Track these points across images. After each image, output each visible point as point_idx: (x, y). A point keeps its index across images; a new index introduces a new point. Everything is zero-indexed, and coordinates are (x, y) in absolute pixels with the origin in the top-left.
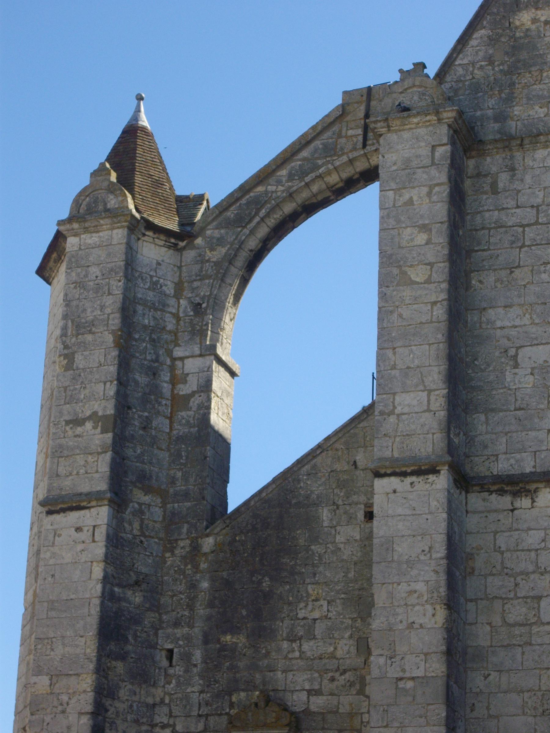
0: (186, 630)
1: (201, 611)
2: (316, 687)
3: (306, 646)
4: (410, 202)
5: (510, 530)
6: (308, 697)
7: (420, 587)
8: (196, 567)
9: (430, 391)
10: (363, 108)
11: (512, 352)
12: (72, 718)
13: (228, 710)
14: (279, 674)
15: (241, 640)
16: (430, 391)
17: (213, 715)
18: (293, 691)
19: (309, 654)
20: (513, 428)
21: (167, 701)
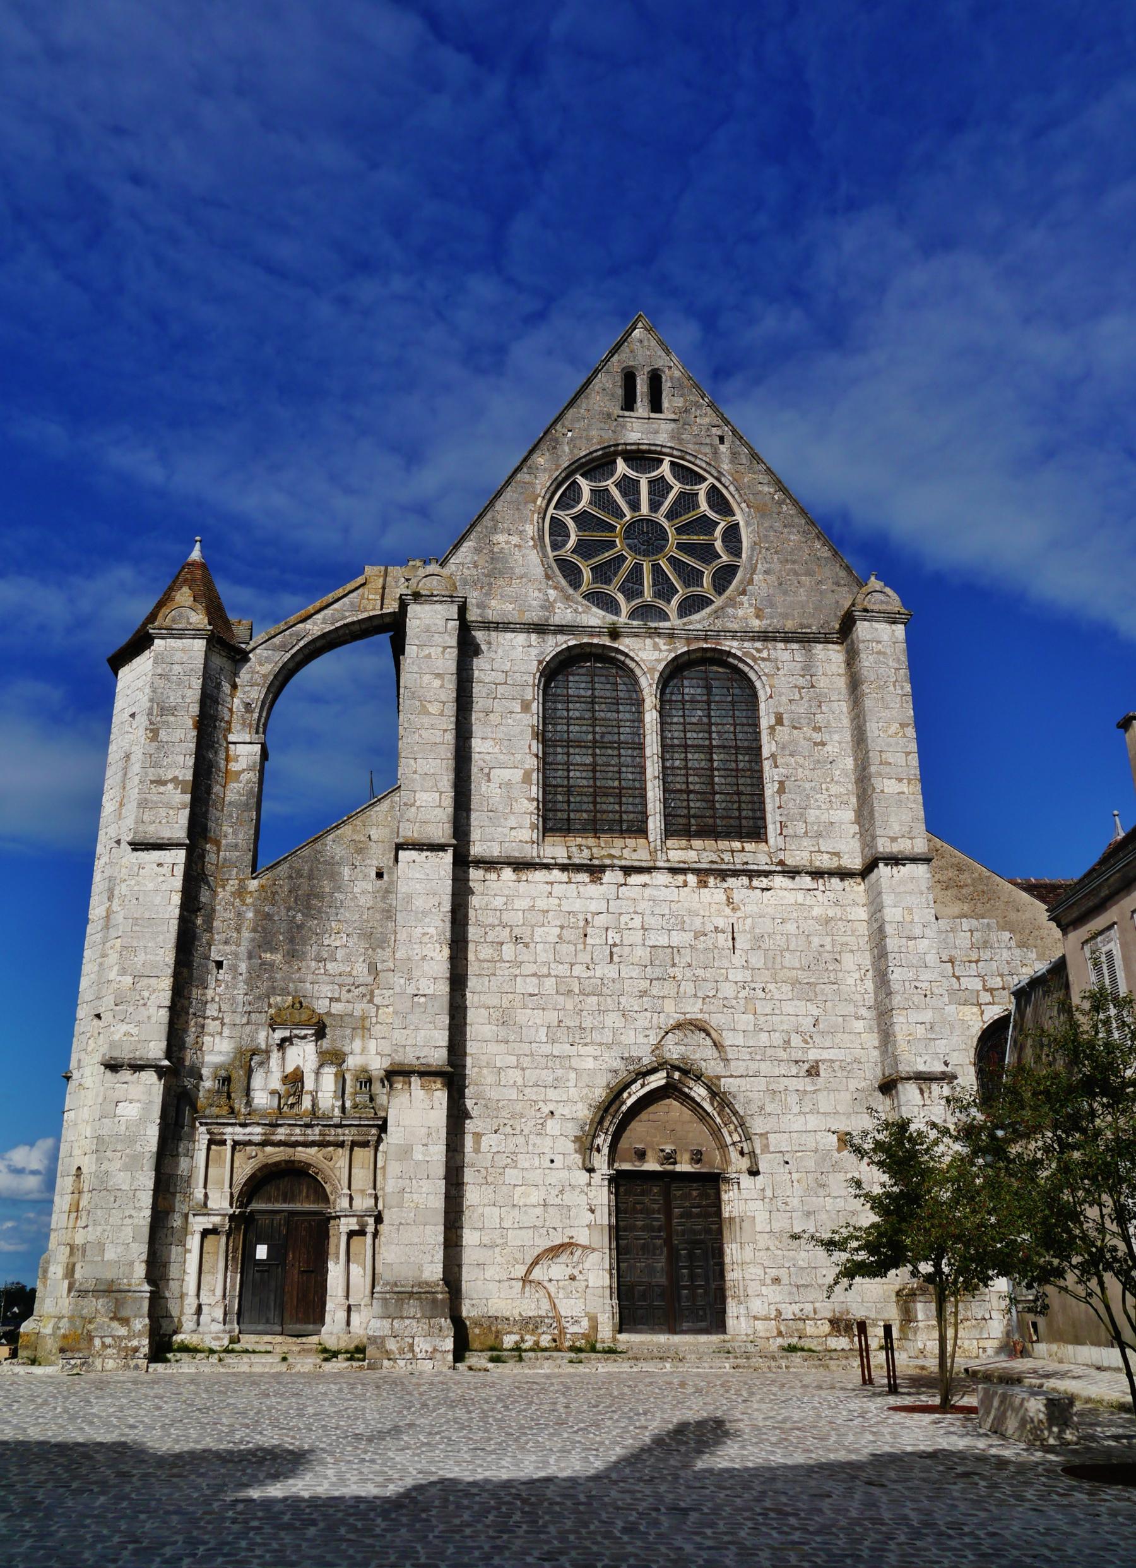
0: (234, 947)
1: (246, 934)
2: (337, 996)
3: (329, 966)
4: (429, 656)
5: (482, 894)
7: (432, 931)
8: (244, 903)
9: (441, 793)
10: (381, 580)
11: (486, 771)
12: (153, 1010)
14: (308, 985)
15: (278, 957)
16: (441, 793)
19: (331, 972)
20: (486, 824)
21: (217, 999)
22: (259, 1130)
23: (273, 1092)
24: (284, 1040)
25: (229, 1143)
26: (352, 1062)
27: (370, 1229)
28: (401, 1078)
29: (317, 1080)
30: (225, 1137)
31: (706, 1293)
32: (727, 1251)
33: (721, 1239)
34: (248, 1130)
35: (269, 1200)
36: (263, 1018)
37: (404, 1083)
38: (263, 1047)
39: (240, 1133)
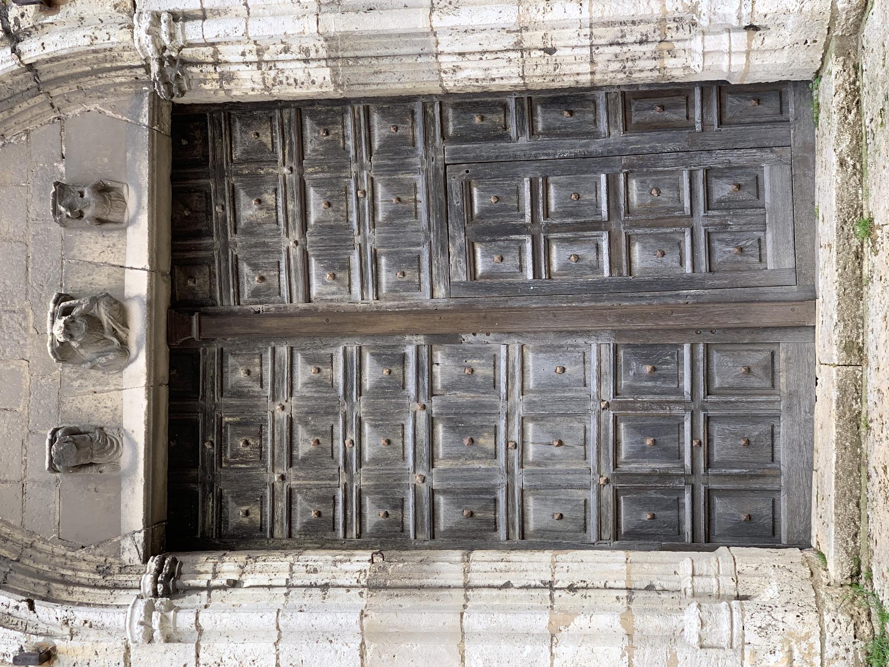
31: (641, 166)
32: (468, 75)
33: (427, 100)
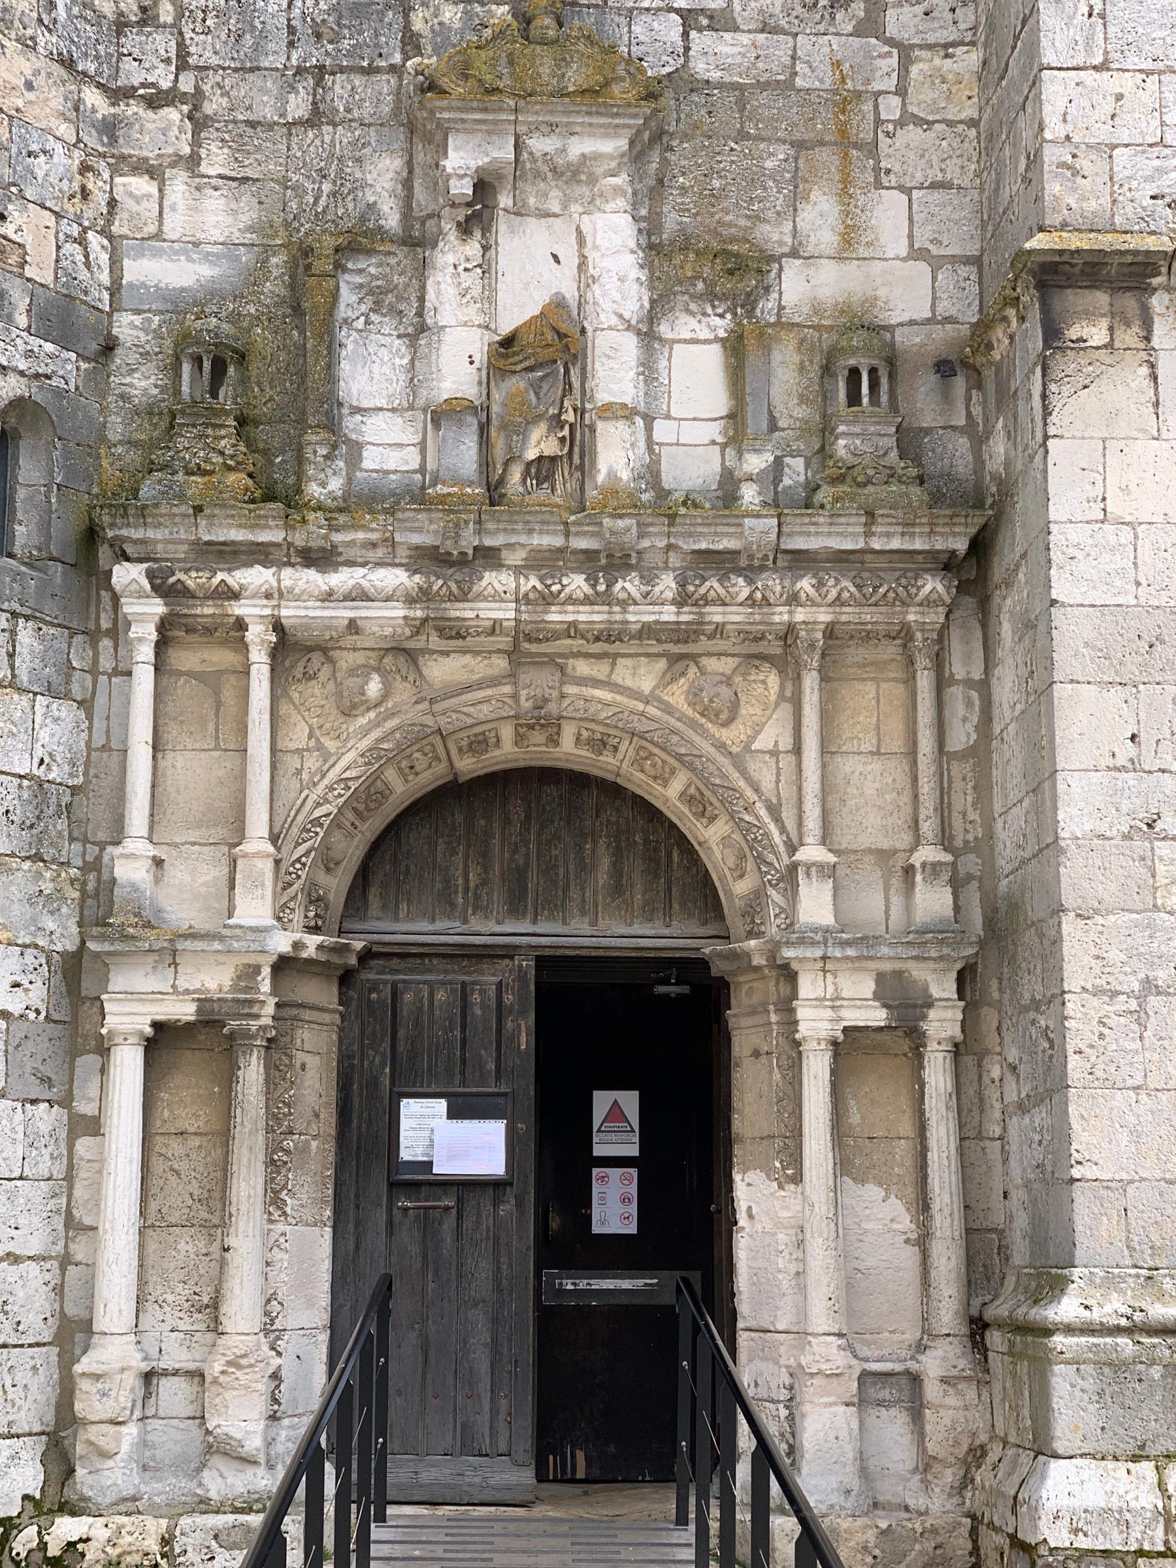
6: (685, 35)
13: (397, 58)
17: (343, 70)
18: (631, 10)
22: (394, 578)
23: (442, 415)
24: (484, 187)
25: (258, 636)
26: (796, 289)
27: (942, 1023)
28: (1102, 298)
29: (648, 370)
30: (239, 609)
34: (342, 579)
35: (446, 903)
36: (374, 96)
37: (1118, 319)
38: (392, 220)
39: (305, 596)
